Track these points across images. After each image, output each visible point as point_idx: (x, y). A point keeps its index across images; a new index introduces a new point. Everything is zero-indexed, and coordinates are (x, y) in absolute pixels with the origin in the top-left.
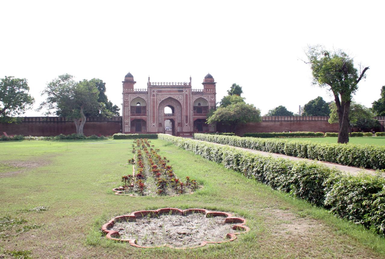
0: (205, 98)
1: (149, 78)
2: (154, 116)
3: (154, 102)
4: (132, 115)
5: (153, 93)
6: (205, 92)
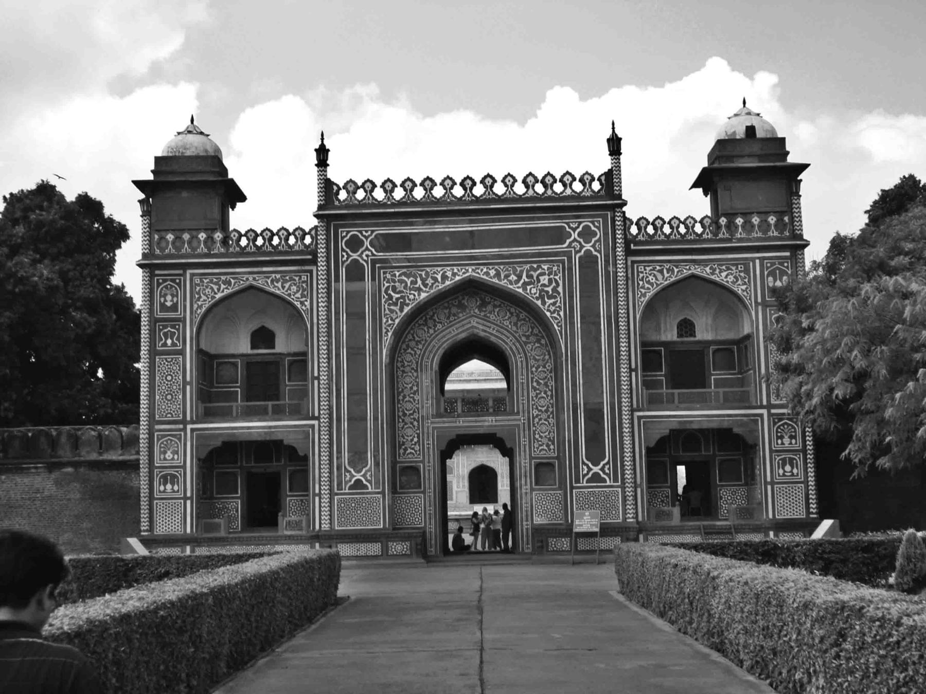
0: (723, 277)
1: (322, 153)
2: (357, 419)
3: (356, 316)
4: (209, 415)
5: (348, 256)
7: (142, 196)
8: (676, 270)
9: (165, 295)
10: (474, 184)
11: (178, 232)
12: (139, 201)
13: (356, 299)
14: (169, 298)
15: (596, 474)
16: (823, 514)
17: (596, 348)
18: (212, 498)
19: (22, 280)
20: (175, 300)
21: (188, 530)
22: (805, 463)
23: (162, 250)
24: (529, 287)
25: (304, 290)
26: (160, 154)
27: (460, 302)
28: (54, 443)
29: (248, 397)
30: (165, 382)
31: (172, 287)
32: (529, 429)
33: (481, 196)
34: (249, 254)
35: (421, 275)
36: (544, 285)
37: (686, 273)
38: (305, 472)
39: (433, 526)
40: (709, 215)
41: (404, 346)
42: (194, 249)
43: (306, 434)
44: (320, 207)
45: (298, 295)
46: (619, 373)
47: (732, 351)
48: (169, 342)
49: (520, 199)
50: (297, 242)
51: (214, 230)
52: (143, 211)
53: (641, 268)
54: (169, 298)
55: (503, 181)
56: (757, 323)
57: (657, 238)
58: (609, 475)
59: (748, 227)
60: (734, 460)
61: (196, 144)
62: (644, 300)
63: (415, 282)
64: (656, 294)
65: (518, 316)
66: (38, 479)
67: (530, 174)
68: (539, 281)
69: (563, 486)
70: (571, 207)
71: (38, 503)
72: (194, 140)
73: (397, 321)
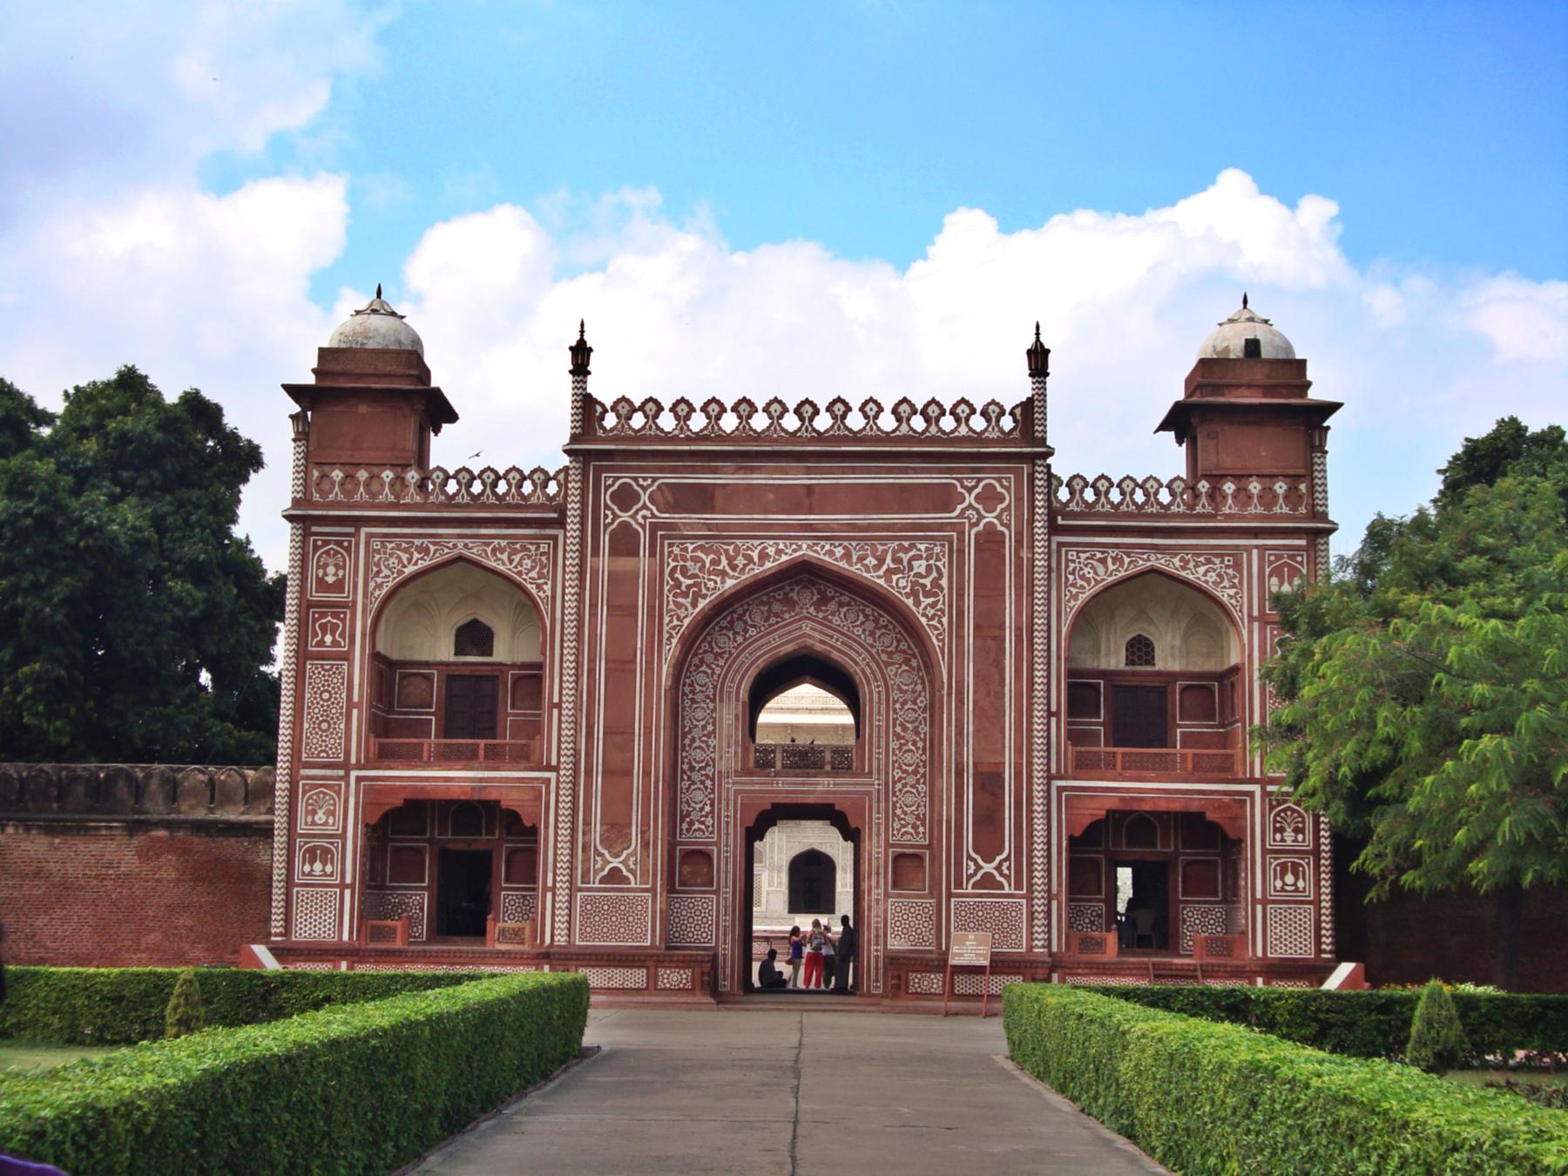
0: (1198, 574)
1: (581, 353)
2: (617, 773)
3: (622, 611)
4: (385, 756)
5: (615, 517)
6: (1204, 506)
7: (296, 409)
8: (1127, 560)
9: (326, 566)
10: (816, 412)
11: (351, 466)
12: (291, 417)
13: (622, 583)
14: (331, 570)
15: (988, 875)
16: (1341, 956)
17: (997, 677)
18: (383, 887)
19: (90, 530)
20: (341, 573)
21: (346, 937)
22: (1317, 873)
23: (324, 494)
24: (894, 578)
25: (543, 567)
26: (326, 345)
27: (786, 595)
28: (139, 790)
29: (447, 731)
30: (319, 699)
31: (336, 552)
32: (887, 801)
33: (827, 431)
34: (459, 506)
35: (727, 551)
37: (1142, 565)
38: (533, 852)
39: (729, 946)
40: (1184, 476)
41: (696, 661)
42: (374, 496)
43: (537, 793)
45: (534, 574)
47: (1209, 690)
48: (328, 639)
49: (888, 438)
50: (534, 491)
51: (406, 466)
52: (297, 433)
53: (1072, 555)
54: (331, 570)
55: (862, 409)
56: (1248, 648)
57: (1099, 508)
58: (1007, 877)
59: (1242, 496)
60: (1208, 862)
61: (383, 331)
62: (1076, 605)
63: (716, 562)
64: (1094, 597)
65: (876, 621)
66: (113, 846)
67: (905, 400)
68: (911, 568)
69: (935, 892)
70: (966, 455)
71: (109, 883)
73: (687, 622)
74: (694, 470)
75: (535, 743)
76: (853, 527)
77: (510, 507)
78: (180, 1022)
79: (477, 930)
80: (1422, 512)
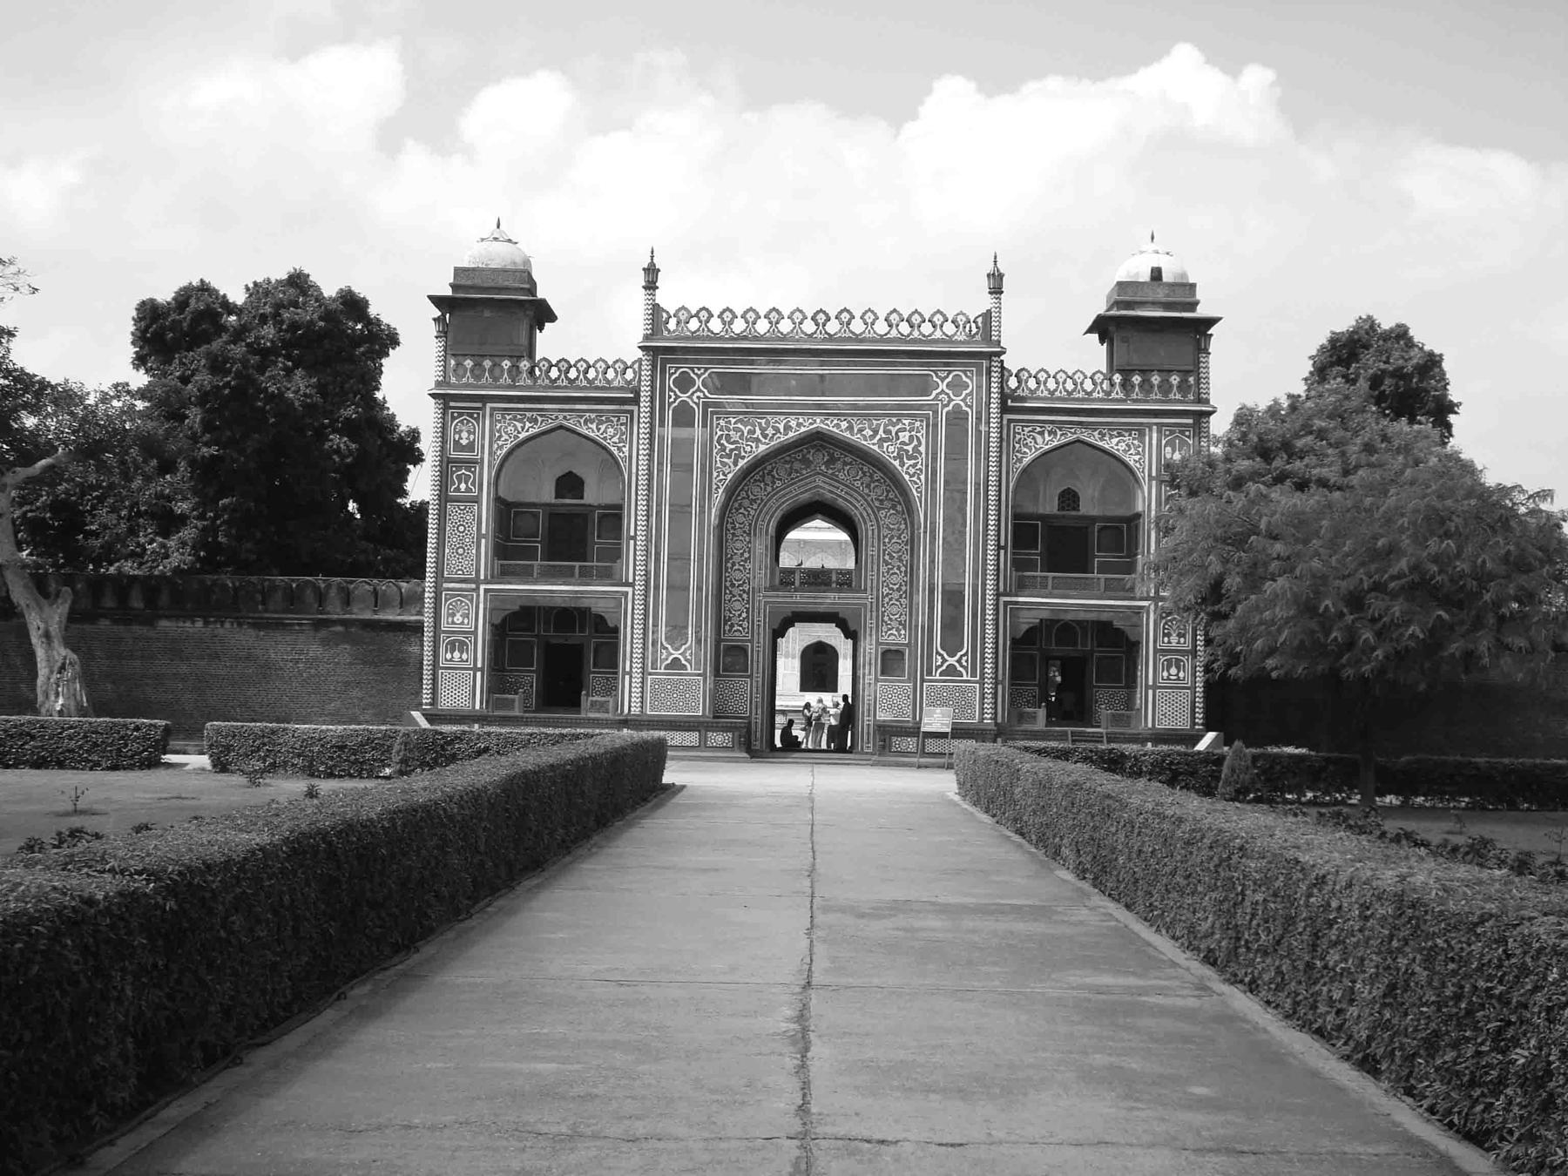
1: (652, 273)
2: (678, 588)
3: (682, 468)
4: (504, 574)
5: (675, 397)
6: (1118, 393)
10: (828, 319)
11: (478, 358)
14: (464, 435)
16: (1209, 729)
17: (959, 517)
18: (504, 670)
23: (459, 377)
28: (321, 597)
34: (559, 387)
36: (903, 443)
42: (496, 379)
43: (618, 599)
44: (646, 338)
45: (615, 439)
46: (985, 550)
48: (463, 486)
49: (882, 339)
51: (520, 357)
54: (464, 435)
57: (1039, 393)
58: (966, 668)
59: (1146, 387)
66: (302, 637)
72: (501, 248)
74: (735, 362)
75: (617, 565)
76: (855, 407)
77: (597, 388)
78: (401, 762)
79: (575, 704)
80: (1276, 401)
